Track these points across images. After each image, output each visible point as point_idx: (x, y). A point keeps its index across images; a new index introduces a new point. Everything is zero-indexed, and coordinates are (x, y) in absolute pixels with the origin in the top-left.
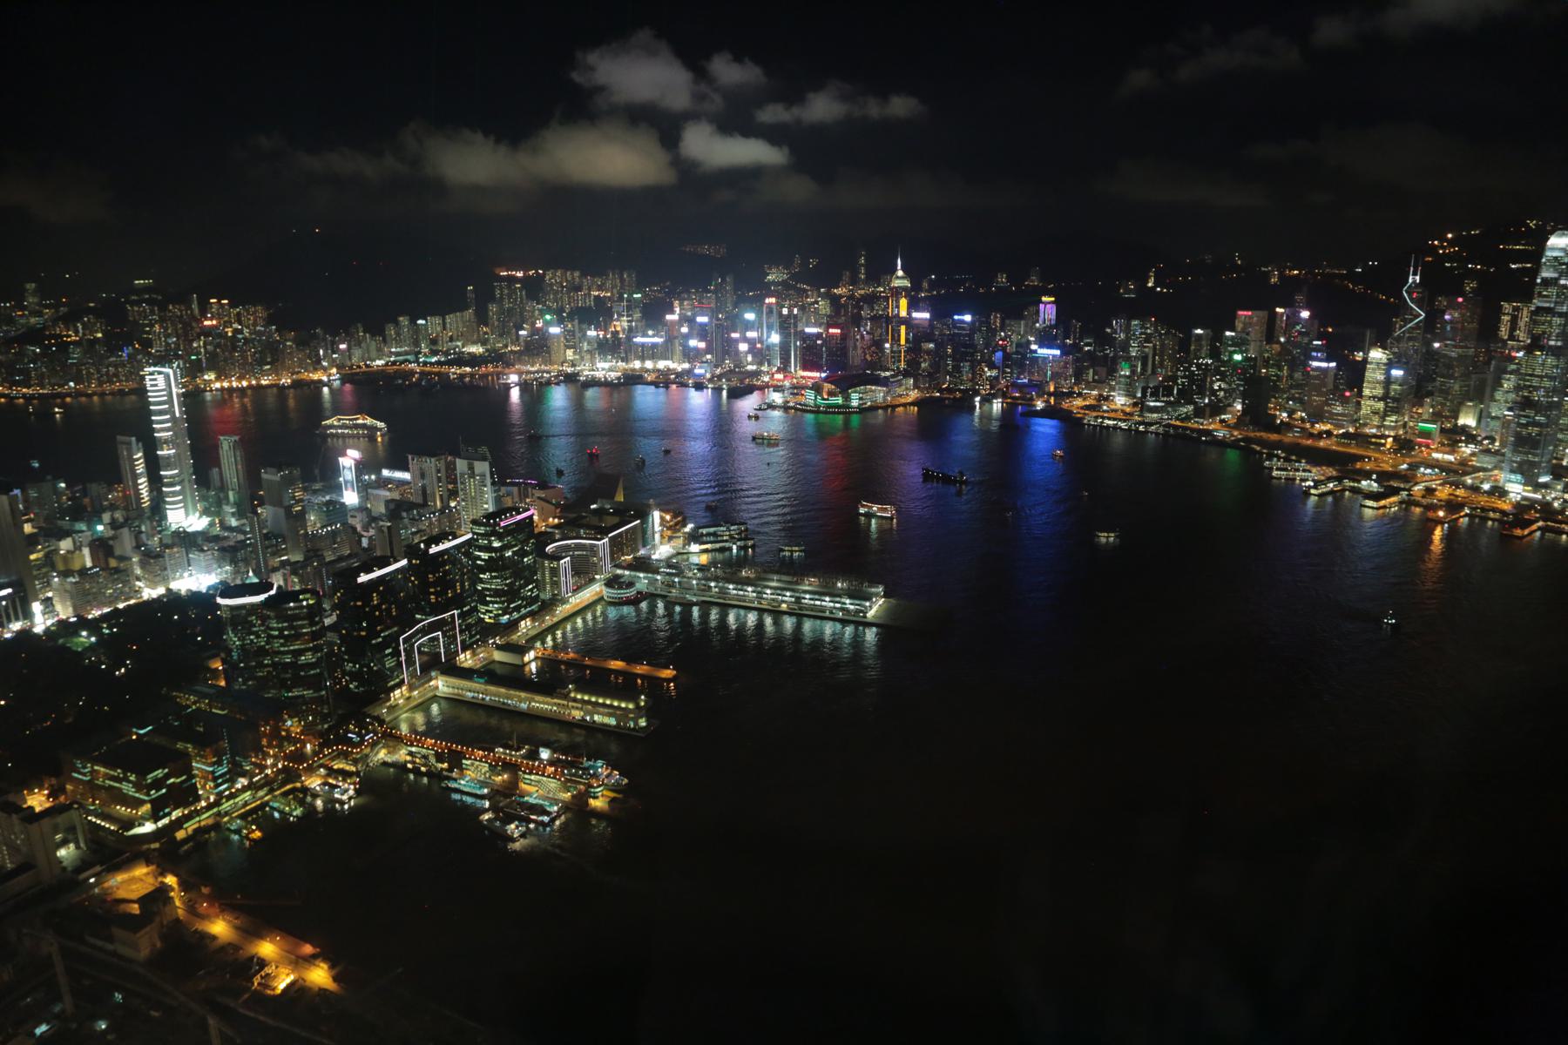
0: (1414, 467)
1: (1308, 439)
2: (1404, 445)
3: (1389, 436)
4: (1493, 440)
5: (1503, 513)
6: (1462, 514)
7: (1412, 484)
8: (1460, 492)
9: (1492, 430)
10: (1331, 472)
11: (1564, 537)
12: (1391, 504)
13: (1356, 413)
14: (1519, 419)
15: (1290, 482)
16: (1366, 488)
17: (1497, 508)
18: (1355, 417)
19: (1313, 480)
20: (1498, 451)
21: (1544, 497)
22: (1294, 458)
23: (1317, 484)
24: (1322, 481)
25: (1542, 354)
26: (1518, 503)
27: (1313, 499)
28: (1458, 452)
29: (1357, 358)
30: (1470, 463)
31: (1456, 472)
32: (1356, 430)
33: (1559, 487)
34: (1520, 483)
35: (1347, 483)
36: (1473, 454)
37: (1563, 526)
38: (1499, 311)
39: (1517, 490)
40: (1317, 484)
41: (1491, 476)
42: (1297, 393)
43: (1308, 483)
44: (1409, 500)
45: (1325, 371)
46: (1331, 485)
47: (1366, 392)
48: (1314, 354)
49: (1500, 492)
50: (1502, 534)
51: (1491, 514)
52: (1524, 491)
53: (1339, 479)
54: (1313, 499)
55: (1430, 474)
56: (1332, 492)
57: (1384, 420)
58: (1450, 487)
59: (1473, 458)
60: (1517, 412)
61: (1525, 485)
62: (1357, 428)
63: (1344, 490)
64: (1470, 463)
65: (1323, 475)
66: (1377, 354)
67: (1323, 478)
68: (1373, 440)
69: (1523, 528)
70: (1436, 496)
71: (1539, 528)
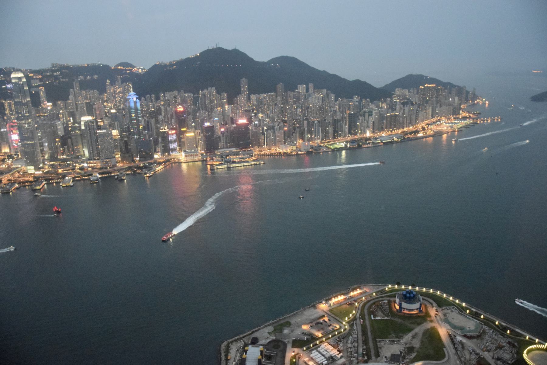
51: (26, 184)
69: (39, 185)
71: (45, 184)
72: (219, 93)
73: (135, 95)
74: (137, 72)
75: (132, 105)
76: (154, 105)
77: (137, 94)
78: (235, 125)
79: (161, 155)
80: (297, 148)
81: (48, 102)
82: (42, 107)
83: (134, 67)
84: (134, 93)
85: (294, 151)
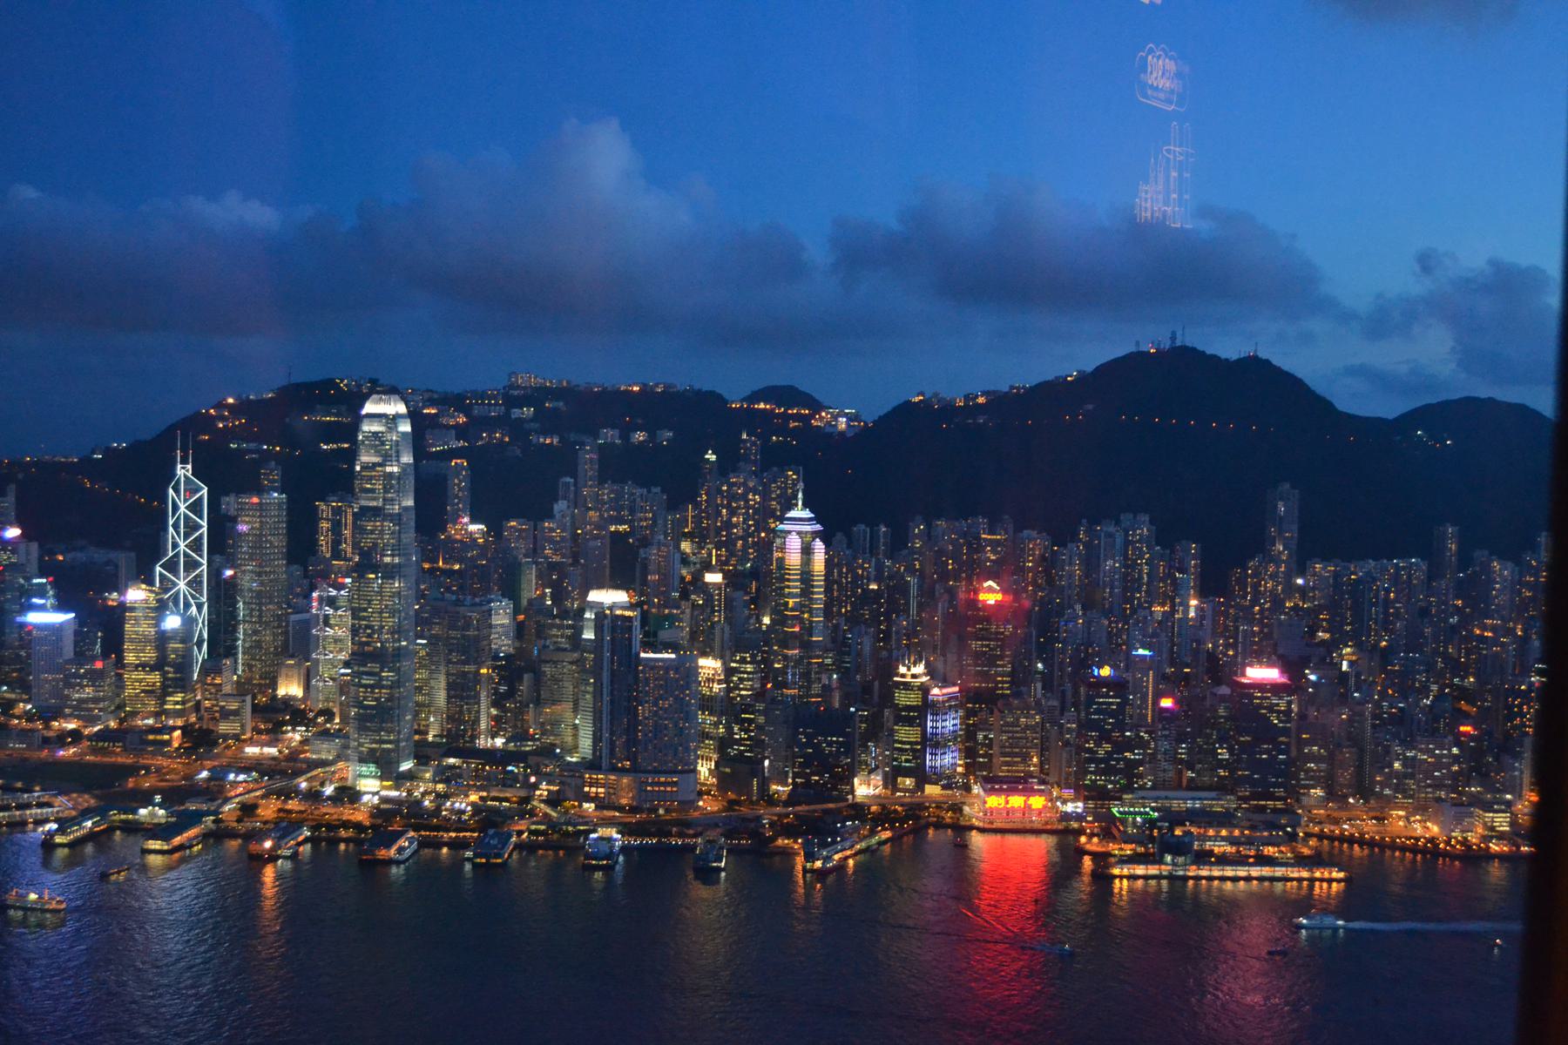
0: (218, 775)
1: (40, 748)
2: (200, 740)
3: (174, 728)
4: (329, 715)
5: (358, 826)
6: (300, 839)
7: (220, 801)
8: (293, 804)
9: (327, 700)
10: (88, 801)
11: (445, 850)
12: (190, 839)
13: (118, 695)
14: (360, 679)
15: (19, 829)
16: (148, 820)
17: (349, 821)
18: (117, 701)
19: (55, 821)
20: (340, 730)
21: (410, 792)
22: (19, 785)
23: (64, 824)
24: (74, 818)
25: (377, 578)
26: (377, 807)
27: (62, 853)
28: (283, 741)
29: (110, 603)
30: (302, 756)
31: (283, 773)
32: (121, 723)
33: (428, 775)
34: (374, 777)
35: (116, 816)
36: (304, 742)
37: (441, 833)
38: (314, 518)
39: (371, 787)
40: (64, 824)
41: (334, 772)
42: (14, 670)
43: (48, 827)
44: (218, 828)
45: (56, 630)
46: (89, 824)
47: (130, 658)
48: (35, 601)
49: (348, 794)
50: (361, 860)
51: (343, 833)
52: (384, 788)
53: (100, 811)
54: (62, 853)
55: (246, 782)
56: (91, 837)
57: (164, 703)
58: (278, 798)
59: (307, 748)
60: (356, 668)
61: (382, 778)
62: (122, 721)
63: (110, 830)
64: (302, 756)
65: (73, 809)
66: (136, 594)
67: (74, 813)
68: (151, 737)
69: (388, 846)
70: (258, 816)
72: (1166, 537)
73: (810, 519)
74: (829, 430)
75: (794, 558)
76: (879, 568)
77: (818, 519)
78: (1224, 690)
79: (885, 786)
80: (1513, 824)
81: (474, 520)
82: (449, 537)
83: (816, 407)
84: (807, 514)
85: (1501, 836)
